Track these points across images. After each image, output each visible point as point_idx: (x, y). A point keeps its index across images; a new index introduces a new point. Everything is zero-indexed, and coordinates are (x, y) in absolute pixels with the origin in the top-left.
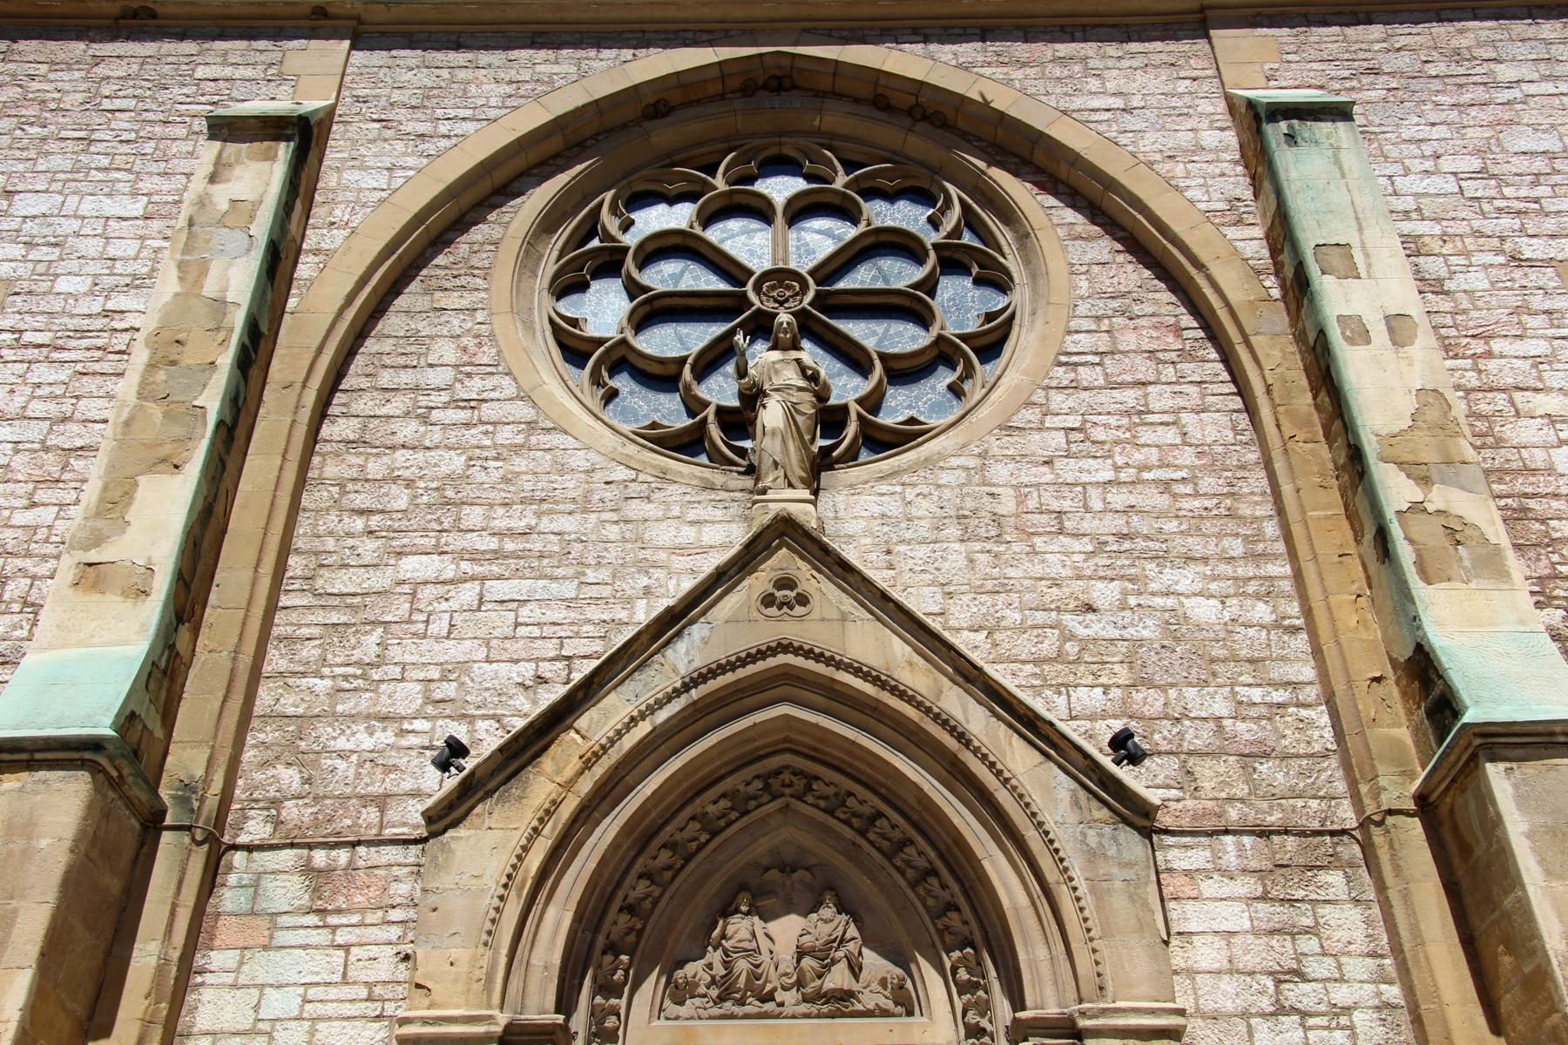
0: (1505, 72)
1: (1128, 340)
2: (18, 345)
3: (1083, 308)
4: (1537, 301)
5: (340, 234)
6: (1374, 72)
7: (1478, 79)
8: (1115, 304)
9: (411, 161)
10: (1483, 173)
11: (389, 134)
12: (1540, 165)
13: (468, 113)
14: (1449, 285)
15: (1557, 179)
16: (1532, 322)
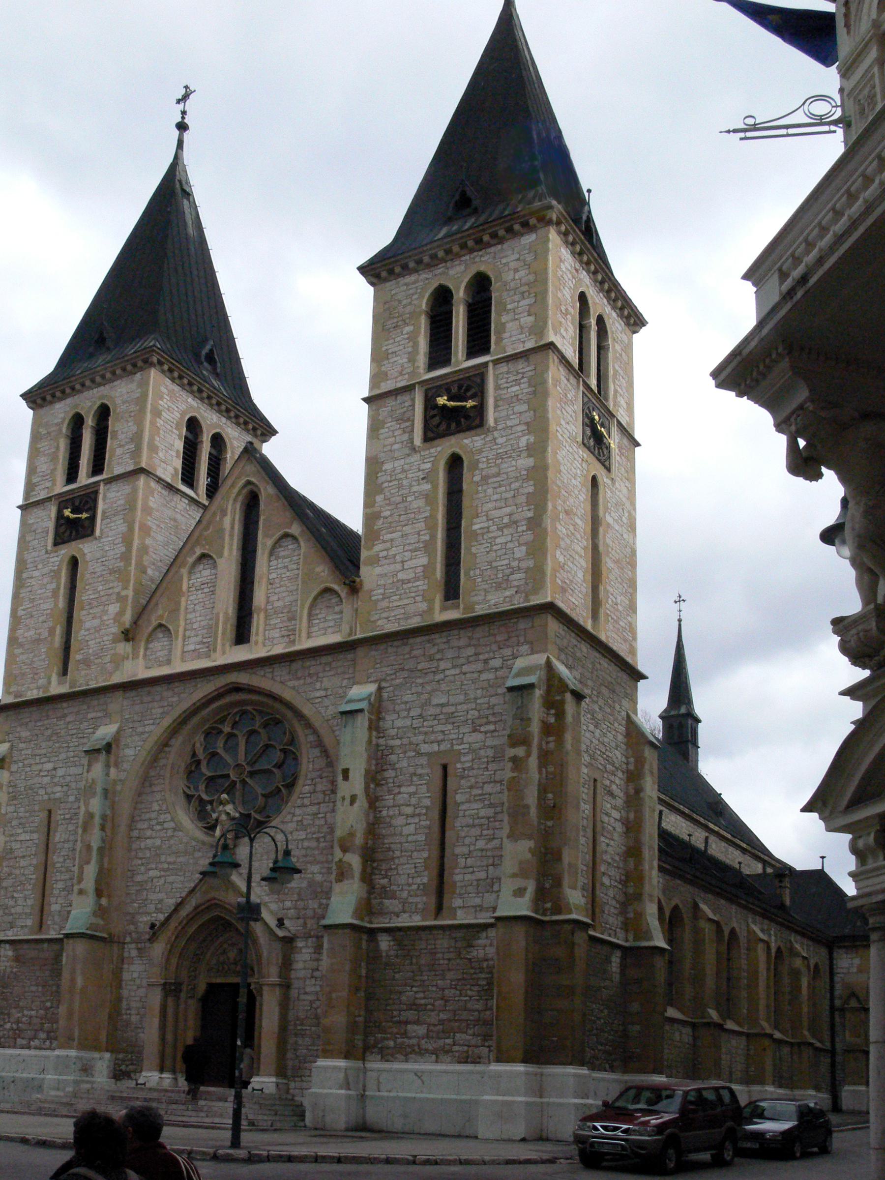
0: (443, 665)
1: (319, 788)
2: (64, 819)
3: (309, 777)
4: (419, 771)
5: (125, 773)
6: (403, 669)
7: (433, 669)
8: (318, 773)
9: (140, 743)
10: (421, 716)
11: (134, 733)
12: (438, 711)
13: (151, 722)
14: (397, 766)
15: (442, 717)
16: (415, 779)
